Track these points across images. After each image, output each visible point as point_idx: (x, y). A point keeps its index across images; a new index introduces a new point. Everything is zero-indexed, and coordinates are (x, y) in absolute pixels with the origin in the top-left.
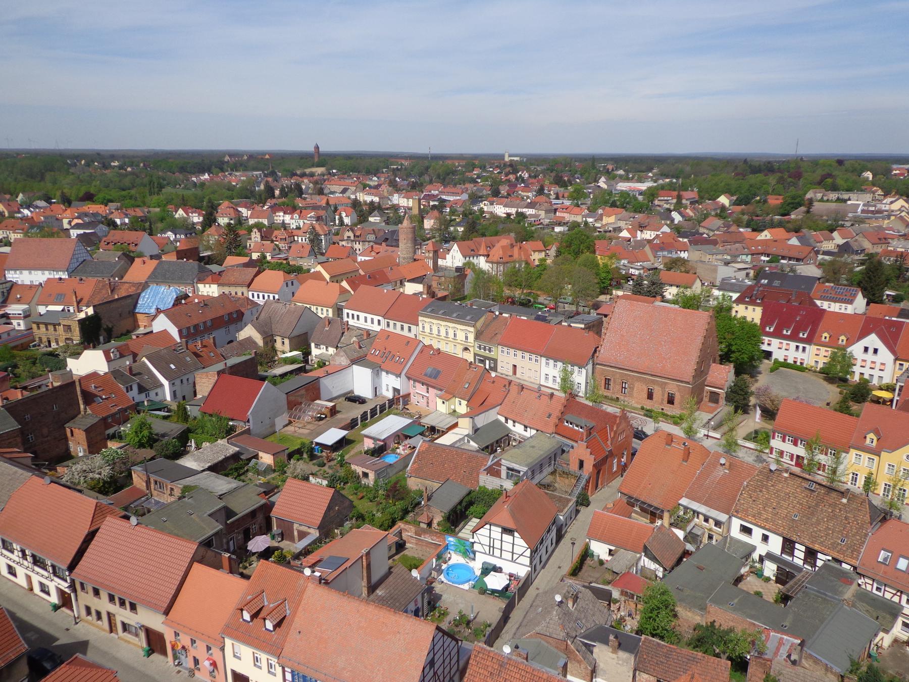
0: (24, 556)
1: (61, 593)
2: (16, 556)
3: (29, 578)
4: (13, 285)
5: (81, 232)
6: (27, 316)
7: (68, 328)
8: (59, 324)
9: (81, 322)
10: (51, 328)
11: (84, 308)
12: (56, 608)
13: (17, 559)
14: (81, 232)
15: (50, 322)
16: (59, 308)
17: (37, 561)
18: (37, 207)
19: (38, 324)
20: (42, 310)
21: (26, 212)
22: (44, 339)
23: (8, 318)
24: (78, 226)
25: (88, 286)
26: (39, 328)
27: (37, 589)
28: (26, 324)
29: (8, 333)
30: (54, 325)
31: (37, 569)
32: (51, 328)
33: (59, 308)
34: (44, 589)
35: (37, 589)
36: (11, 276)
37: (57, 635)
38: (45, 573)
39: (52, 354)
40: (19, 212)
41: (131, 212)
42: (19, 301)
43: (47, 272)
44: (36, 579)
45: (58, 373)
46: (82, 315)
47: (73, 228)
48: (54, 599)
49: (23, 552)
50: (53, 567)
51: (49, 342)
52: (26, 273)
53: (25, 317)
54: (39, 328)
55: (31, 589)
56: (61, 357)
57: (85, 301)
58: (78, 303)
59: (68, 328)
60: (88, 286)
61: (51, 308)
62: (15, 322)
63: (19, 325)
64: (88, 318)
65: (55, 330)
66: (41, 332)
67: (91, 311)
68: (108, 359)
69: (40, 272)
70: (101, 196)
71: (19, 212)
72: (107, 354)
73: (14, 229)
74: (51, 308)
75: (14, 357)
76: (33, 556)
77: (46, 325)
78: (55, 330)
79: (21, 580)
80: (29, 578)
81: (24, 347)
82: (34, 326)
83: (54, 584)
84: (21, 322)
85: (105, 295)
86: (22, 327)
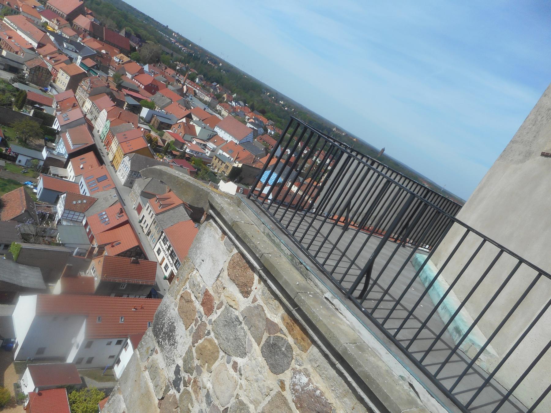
0: (168, 249)
1: (172, 273)
2: (165, 247)
3: (164, 259)
4: (216, 135)
5: (252, 127)
6: (213, 151)
7: (227, 167)
8: (225, 163)
9: (234, 168)
10: (220, 162)
11: (237, 162)
12: (165, 278)
13: (165, 249)
14: (252, 127)
15: (221, 160)
16: (228, 156)
17: (172, 255)
18: (239, 104)
19: (217, 157)
20: (220, 151)
21: (234, 104)
22: (214, 166)
23: (206, 147)
24: (251, 123)
25: (245, 154)
26: (216, 159)
27: (163, 266)
28: (210, 154)
29: (202, 154)
30: (223, 162)
31: (169, 257)
32: (220, 162)
33: (228, 156)
34: (166, 267)
35: (163, 266)
36: (217, 129)
37: (160, 289)
38: (172, 262)
39: (215, 174)
40: (231, 102)
41: (277, 130)
42: (214, 143)
43: (231, 137)
44: (166, 261)
45: (214, 184)
46: (236, 165)
47: (249, 123)
48: (167, 274)
49: (169, 247)
50: (177, 261)
51: (216, 167)
52: (223, 132)
53: (212, 151)
54: (216, 159)
55: (161, 264)
56: (217, 178)
57: (239, 160)
58: (236, 159)
59: (227, 167)
60: (245, 154)
61: (224, 153)
62: (207, 150)
63: (208, 153)
64: (237, 168)
65: (221, 164)
66: (215, 162)
67: (240, 165)
68: (237, 191)
69: (229, 135)
70: (269, 114)
71: (231, 102)
72: (238, 189)
73: (226, 109)
74: (224, 153)
75: (200, 165)
76: (172, 251)
77: (220, 160)
78: (221, 164)
79: (160, 258)
80: (164, 259)
81: (205, 164)
82: (215, 157)
83: (172, 268)
84: (209, 152)
85: (249, 162)
86: (208, 155)
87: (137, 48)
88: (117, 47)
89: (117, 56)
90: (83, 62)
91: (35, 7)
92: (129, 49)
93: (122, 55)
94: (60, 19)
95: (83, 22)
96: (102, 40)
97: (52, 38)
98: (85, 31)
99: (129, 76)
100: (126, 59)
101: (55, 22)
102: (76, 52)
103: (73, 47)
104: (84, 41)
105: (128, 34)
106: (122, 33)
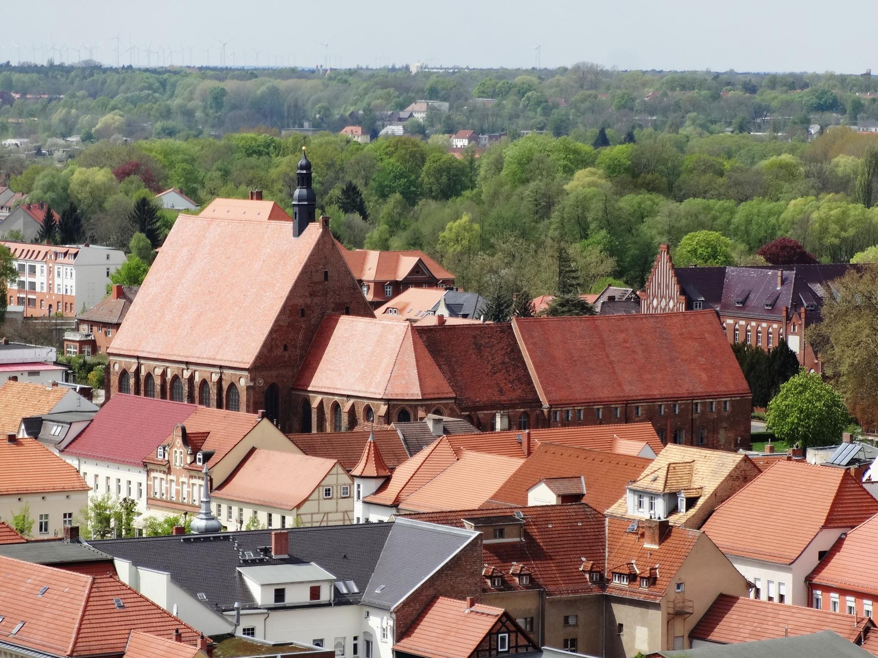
87: (794, 343)
88: (623, 413)
89: (644, 482)
90: (407, 645)
91: (34, 425)
92: (733, 380)
93: (674, 453)
94: (205, 418)
95: (366, 359)
96: (529, 415)
97: (155, 585)
98: (401, 411)
99: (777, 584)
100: (709, 467)
101: (179, 455)
102: (340, 600)
103: (314, 572)
104: (389, 495)
105: (702, 285)
106: (663, 295)
